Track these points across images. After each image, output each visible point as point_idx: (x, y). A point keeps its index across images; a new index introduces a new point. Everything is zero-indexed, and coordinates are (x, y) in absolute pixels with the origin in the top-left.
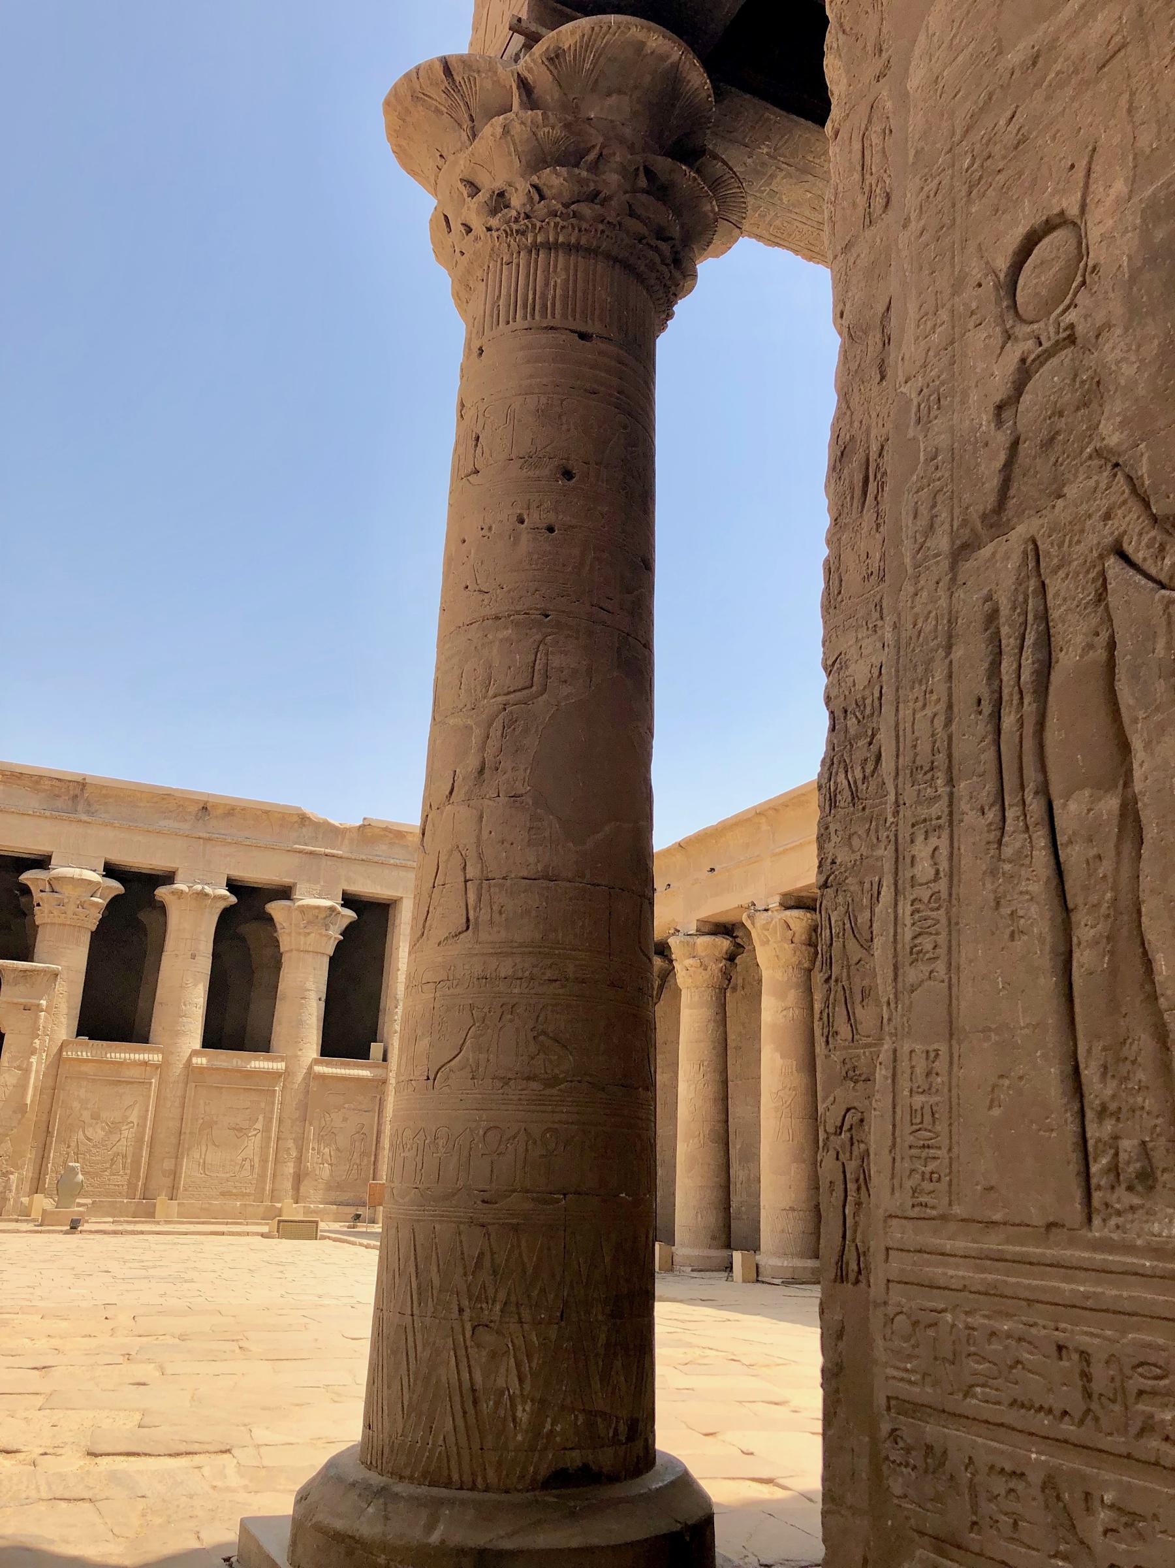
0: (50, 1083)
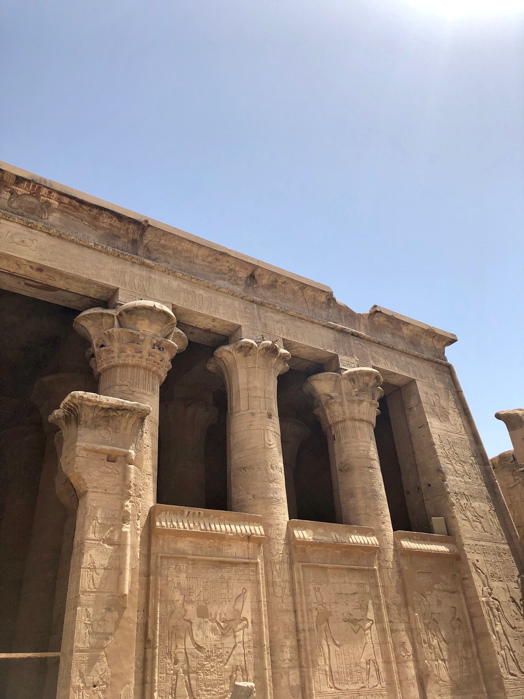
0: (144, 567)
